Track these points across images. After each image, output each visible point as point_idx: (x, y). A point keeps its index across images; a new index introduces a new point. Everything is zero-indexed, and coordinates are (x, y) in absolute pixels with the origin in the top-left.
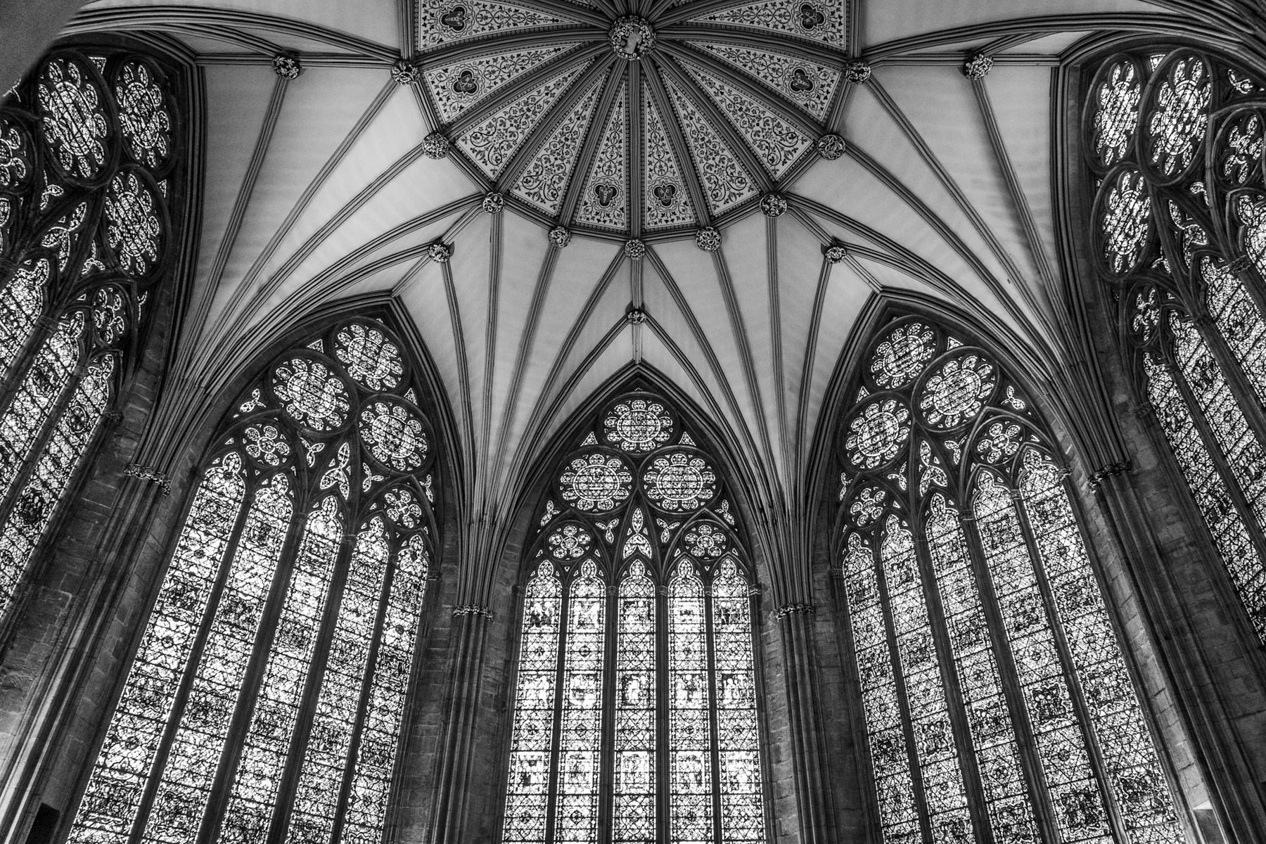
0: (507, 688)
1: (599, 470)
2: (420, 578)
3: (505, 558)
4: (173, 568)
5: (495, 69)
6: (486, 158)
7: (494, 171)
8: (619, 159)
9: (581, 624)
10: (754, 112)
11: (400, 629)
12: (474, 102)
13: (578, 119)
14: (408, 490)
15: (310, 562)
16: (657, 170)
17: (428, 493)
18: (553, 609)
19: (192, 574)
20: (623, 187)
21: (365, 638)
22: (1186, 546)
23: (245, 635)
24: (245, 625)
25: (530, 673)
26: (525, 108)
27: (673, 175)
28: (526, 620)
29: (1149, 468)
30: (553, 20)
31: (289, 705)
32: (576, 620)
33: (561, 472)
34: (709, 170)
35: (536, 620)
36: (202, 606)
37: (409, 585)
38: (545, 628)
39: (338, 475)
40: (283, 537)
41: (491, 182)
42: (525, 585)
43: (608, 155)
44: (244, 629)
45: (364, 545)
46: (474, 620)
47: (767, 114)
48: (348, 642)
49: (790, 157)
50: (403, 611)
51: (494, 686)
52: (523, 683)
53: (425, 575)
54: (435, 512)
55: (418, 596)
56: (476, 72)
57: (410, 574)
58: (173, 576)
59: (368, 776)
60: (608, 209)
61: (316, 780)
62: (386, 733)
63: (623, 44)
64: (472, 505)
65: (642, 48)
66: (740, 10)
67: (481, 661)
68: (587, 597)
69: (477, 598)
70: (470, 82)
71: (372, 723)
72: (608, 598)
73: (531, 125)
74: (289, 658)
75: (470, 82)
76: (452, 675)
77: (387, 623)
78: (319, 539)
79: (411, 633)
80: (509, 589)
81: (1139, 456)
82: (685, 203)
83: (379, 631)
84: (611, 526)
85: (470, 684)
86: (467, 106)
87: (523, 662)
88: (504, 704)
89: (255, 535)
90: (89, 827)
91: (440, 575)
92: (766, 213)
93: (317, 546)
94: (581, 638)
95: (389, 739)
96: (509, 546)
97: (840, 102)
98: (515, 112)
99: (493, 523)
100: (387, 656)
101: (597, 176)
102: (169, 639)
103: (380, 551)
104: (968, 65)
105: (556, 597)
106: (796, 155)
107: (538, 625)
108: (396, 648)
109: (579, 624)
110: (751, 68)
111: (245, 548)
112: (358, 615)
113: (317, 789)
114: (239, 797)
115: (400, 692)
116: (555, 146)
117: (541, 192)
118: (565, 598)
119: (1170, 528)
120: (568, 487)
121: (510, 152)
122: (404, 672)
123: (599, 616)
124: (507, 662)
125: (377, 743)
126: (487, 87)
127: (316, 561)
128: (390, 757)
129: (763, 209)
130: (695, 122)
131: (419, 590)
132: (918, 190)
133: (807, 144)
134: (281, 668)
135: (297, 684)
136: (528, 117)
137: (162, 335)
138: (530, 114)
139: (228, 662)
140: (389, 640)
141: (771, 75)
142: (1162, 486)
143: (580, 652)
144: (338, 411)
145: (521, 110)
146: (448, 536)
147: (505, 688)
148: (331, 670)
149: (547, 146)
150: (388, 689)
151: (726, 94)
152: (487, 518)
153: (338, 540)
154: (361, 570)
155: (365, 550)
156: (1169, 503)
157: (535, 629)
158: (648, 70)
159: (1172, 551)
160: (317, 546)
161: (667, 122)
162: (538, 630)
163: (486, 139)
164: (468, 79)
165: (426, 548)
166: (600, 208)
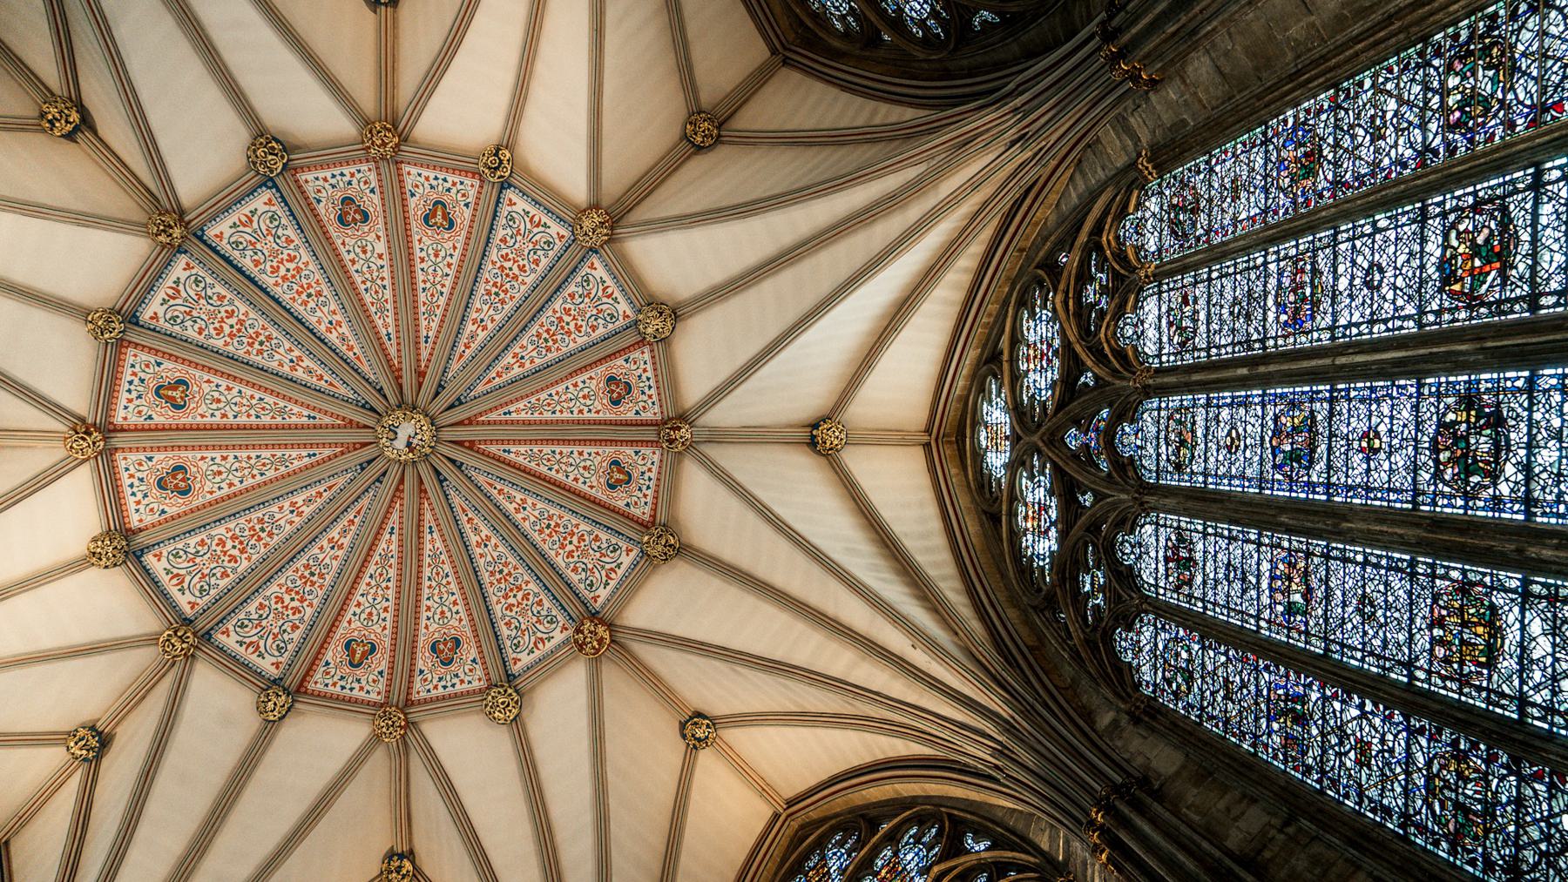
8: (385, 604)
10: (565, 527)
22: (1280, 831)
27: (459, 623)
29: (1172, 770)
30: (309, 417)
34: (508, 613)
43: (370, 598)
47: (582, 527)
49: (613, 575)
60: (358, 672)
63: (391, 435)
65: (415, 441)
66: (538, 400)
81: (1154, 764)
82: (474, 661)
92: (581, 647)
97: (668, 486)
101: (353, 625)
104: (815, 432)
106: (620, 572)
110: (558, 472)
119: (1241, 824)
129: (576, 641)
130: (490, 551)
132: (778, 580)
133: (632, 555)
141: (582, 475)
142: (1202, 777)
151: (530, 511)
156: (1225, 789)
158: (430, 483)
159: (1259, 852)
161: (451, 547)
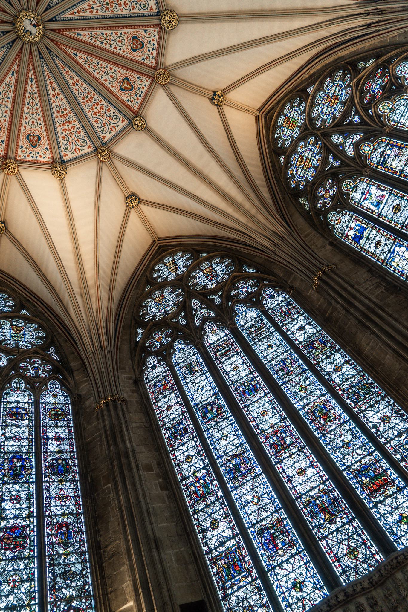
0: (386, 279)
1: (300, 159)
2: (286, 300)
3: (310, 241)
4: (162, 426)
5: (31, 120)
6: (80, 148)
7: (89, 147)
9: (377, 205)
11: (301, 328)
12: (46, 141)
13: (77, 85)
14: (238, 281)
15: (223, 355)
16: (120, 45)
17: (251, 271)
18: (358, 222)
19: (173, 419)
20: (126, 72)
21: (286, 351)
23: (224, 416)
24: (219, 412)
25: (388, 257)
26: (61, 114)
28: (353, 245)
31: (280, 422)
32: (373, 208)
33: (288, 185)
35: (357, 239)
36: (190, 426)
37: (283, 309)
38: (366, 233)
39: (201, 313)
40: (201, 360)
41: (95, 151)
42: (333, 235)
44: (220, 414)
45: (242, 320)
46: (325, 278)
48: (280, 363)
50: (293, 320)
51: (377, 287)
52: (391, 266)
53: (287, 297)
54: (261, 273)
55: (294, 307)
56: (29, 132)
57: (278, 304)
58: (166, 429)
59: (368, 407)
61: (339, 441)
62: (353, 376)
64: (266, 247)
67: (353, 287)
68: (363, 194)
69: (314, 269)
70: (34, 137)
71: (338, 381)
72: (371, 177)
73: (72, 115)
74: (256, 402)
75: (34, 137)
76: (347, 311)
77: (291, 334)
78: (218, 342)
79: (309, 324)
80: (328, 247)
83: (290, 341)
84: (332, 161)
85: (360, 301)
86: (47, 145)
87: (378, 260)
88: (395, 287)
89: (187, 374)
90: (232, 593)
91: (292, 287)
93: (220, 345)
94: (386, 209)
95: (358, 378)
96: (306, 236)
98: (61, 120)
99: (282, 238)
100: (308, 345)
102: (188, 457)
103: (252, 314)
105: (351, 217)
107: (361, 238)
108: (309, 337)
109: (376, 206)
111: (187, 383)
112: (271, 347)
113: (346, 445)
114: (302, 494)
115: (337, 351)
116: (88, 106)
117: (112, 125)
118: (355, 210)
120: (298, 186)
121: (83, 134)
122: (327, 341)
123: (380, 189)
124: (370, 271)
125: (354, 386)
126: (40, 129)
127: (225, 352)
128: (370, 385)
131: (291, 304)
134: (257, 410)
135: (274, 408)
136: (66, 114)
137: (73, 353)
138: (65, 113)
139: (227, 436)
140: (301, 339)
143: (395, 213)
144: (177, 296)
145: (61, 116)
146: (277, 271)
147: (385, 280)
148: (285, 383)
149: (87, 110)
150: (328, 357)
152: (276, 241)
153: (227, 333)
154: (252, 330)
155: (245, 321)
157: (362, 242)
160: (220, 345)
162: (364, 239)
163: (70, 143)
164: (32, 138)
165: (273, 287)
166: (133, 92)
